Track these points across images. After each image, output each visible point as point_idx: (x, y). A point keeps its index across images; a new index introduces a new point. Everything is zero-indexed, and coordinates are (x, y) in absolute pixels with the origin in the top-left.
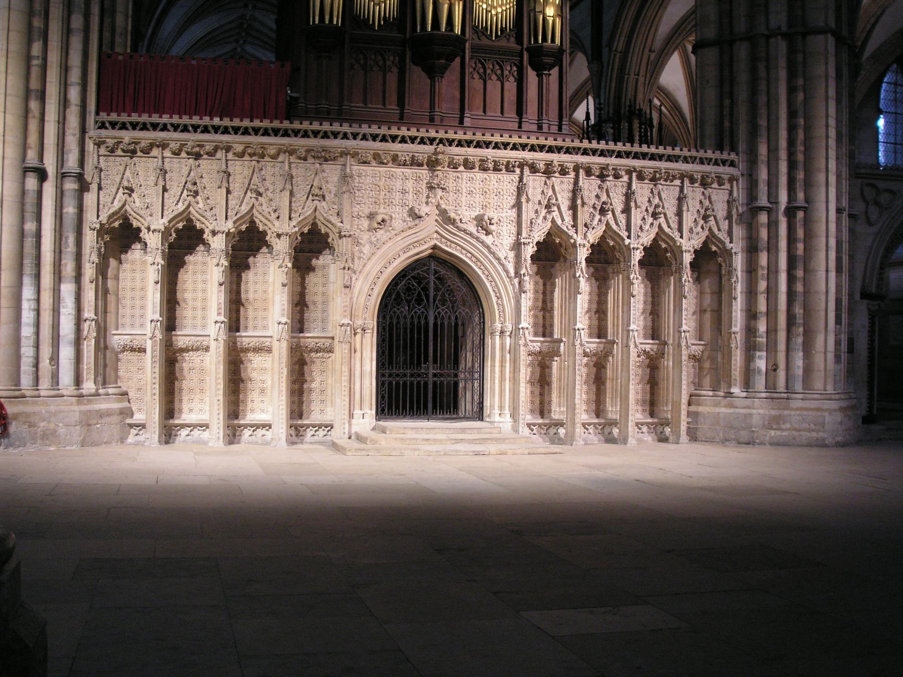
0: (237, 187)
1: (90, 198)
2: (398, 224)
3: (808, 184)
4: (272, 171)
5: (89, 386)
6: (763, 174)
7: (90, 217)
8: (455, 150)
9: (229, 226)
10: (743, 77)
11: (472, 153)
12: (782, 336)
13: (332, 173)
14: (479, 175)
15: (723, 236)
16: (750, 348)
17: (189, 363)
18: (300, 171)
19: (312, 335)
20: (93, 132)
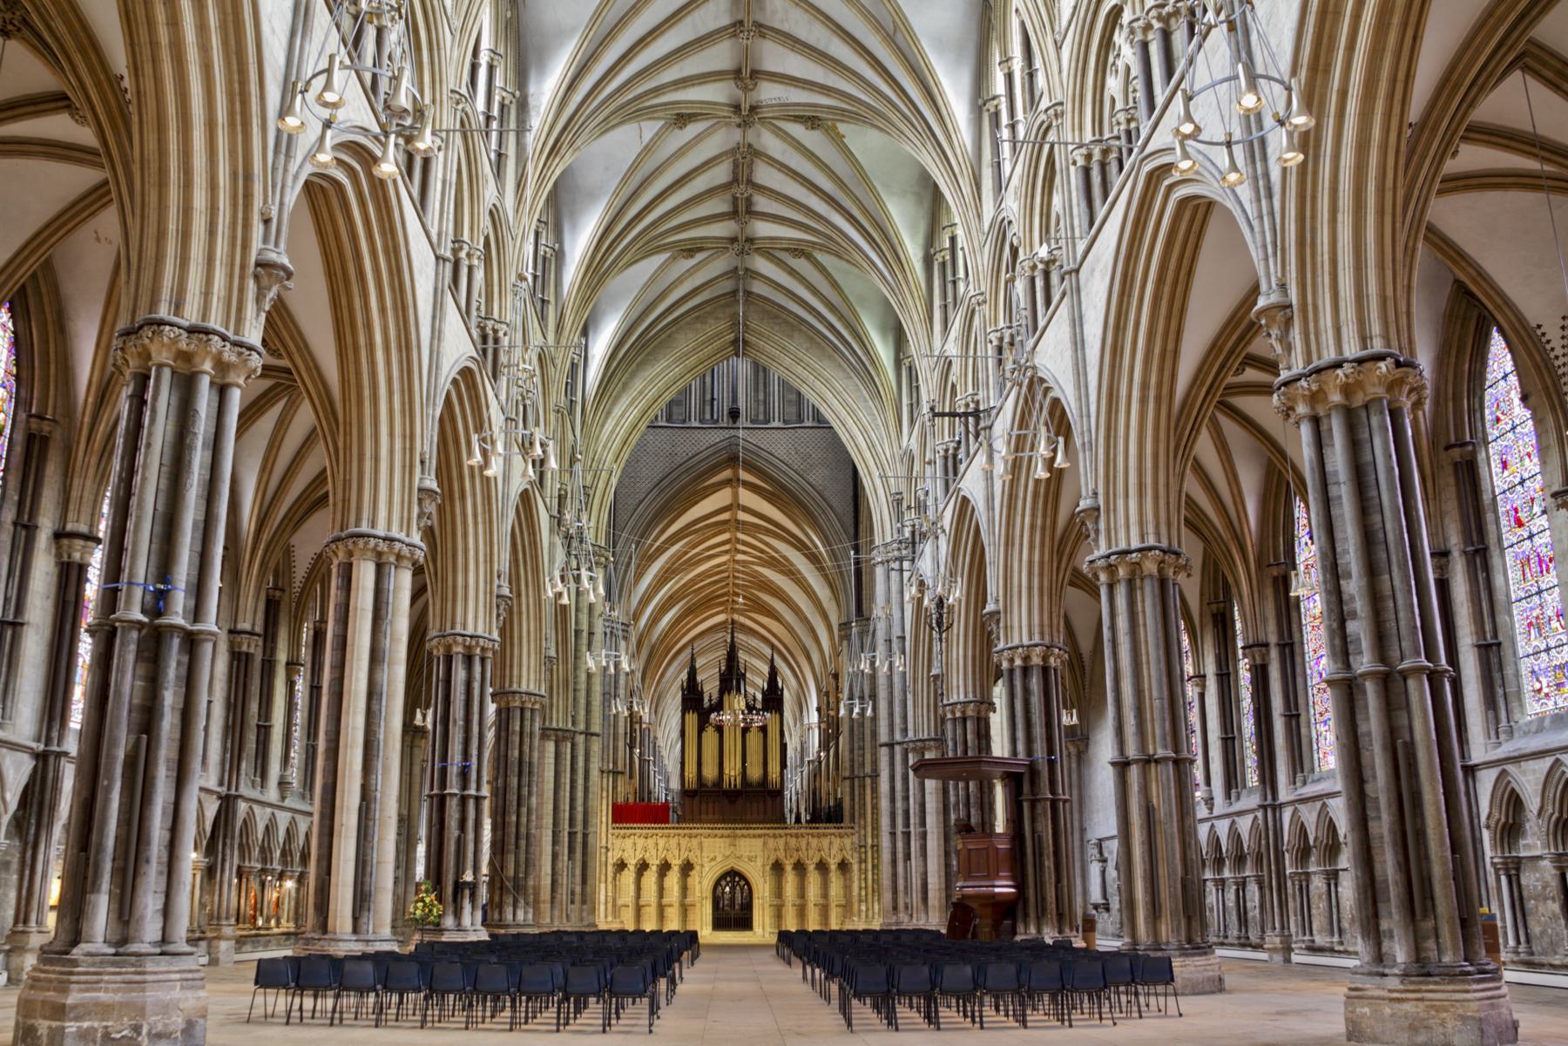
0: (661, 846)
1: (610, 854)
2: (719, 859)
3: (877, 836)
4: (673, 842)
5: (610, 919)
6: (863, 832)
7: (610, 861)
8: (738, 832)
9: (658, 862)
10: (857, 792)
11: (744, 832)
12: (870, 896)
13: (695, 842)
14: (748, 840)
15: (848, 857)
16: (860, 901)
17: (644, 911)
18: (684, 842)
19: (689, 900)
20: (610, 831)
